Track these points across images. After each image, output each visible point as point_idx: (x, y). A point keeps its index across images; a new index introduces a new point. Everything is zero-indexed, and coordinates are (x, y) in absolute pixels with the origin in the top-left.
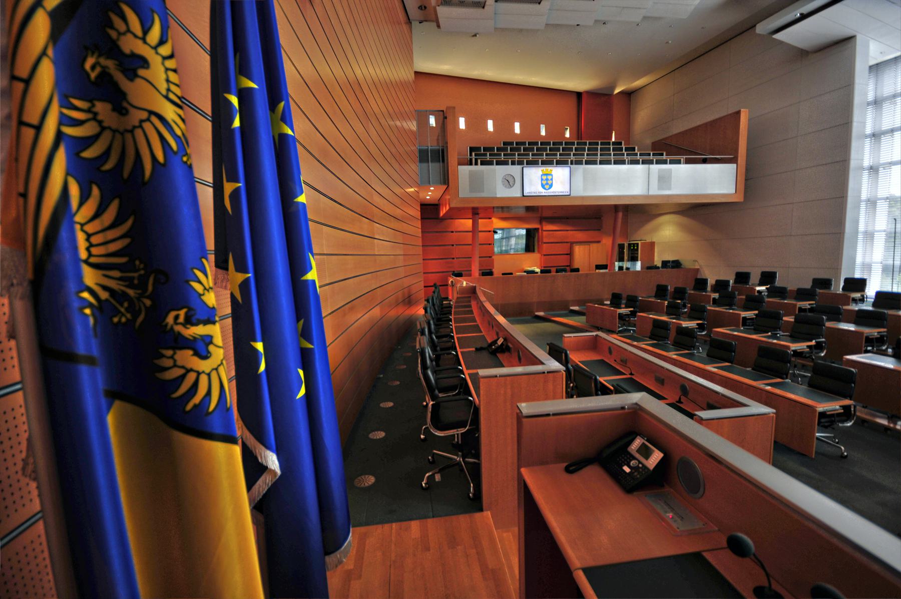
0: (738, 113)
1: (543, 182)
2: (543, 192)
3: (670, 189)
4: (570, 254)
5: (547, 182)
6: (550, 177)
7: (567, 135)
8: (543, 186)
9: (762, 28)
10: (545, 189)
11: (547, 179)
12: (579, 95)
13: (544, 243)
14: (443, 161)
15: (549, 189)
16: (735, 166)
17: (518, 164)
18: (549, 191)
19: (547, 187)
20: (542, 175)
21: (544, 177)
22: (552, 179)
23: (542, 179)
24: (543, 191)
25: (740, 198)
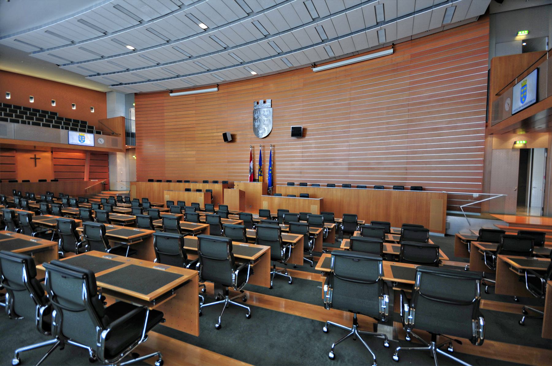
1: (80, 139)
2: (80, 143)
5: (82, 139)
6: (83, 137)
8: (80, 141)
10: (81, 142)
11: (82, 138)
15: (83, 142)
18: (83, 143)
19: (82, 141)
20: (79, 136)
21: (80, 137)
22: (84, 138)
23: (79, 138)
24: (80, 143)
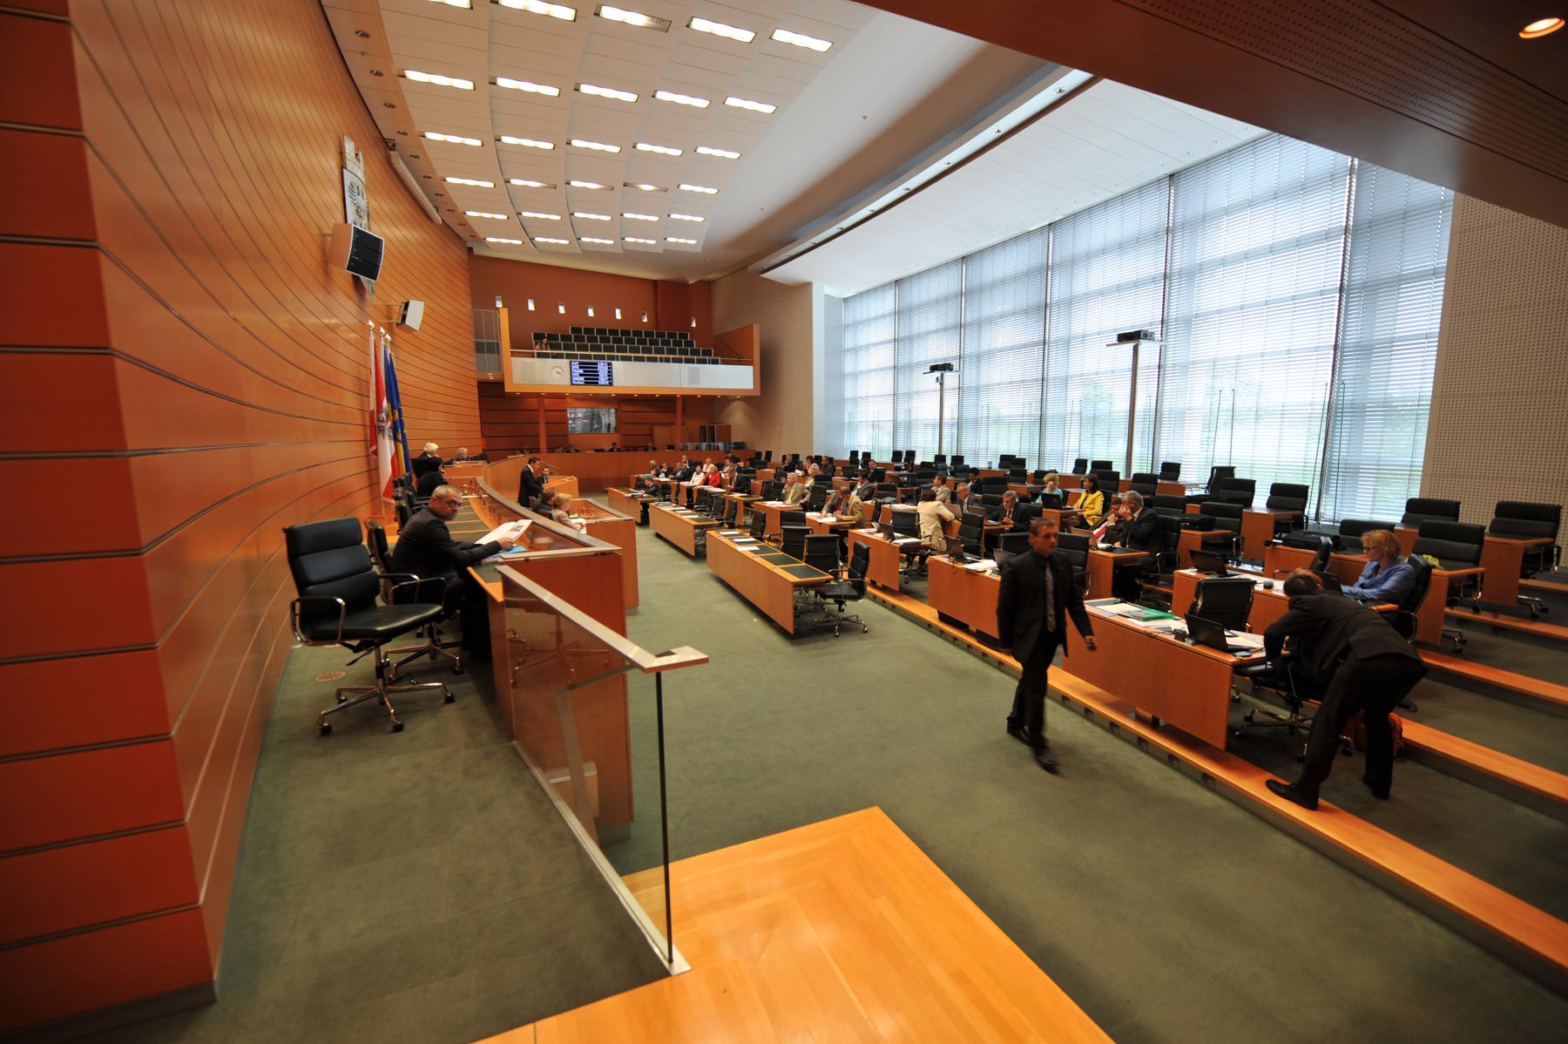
0: (752, 326)
3: (698, 383)
4: (651, 435)
7: (645, 320)
9: (750, 269)
12: (655, 282)
13: (624, 423)
14: (498, 352)
16: (750, 368)
17: (567, 358)
25: (758, 393)
